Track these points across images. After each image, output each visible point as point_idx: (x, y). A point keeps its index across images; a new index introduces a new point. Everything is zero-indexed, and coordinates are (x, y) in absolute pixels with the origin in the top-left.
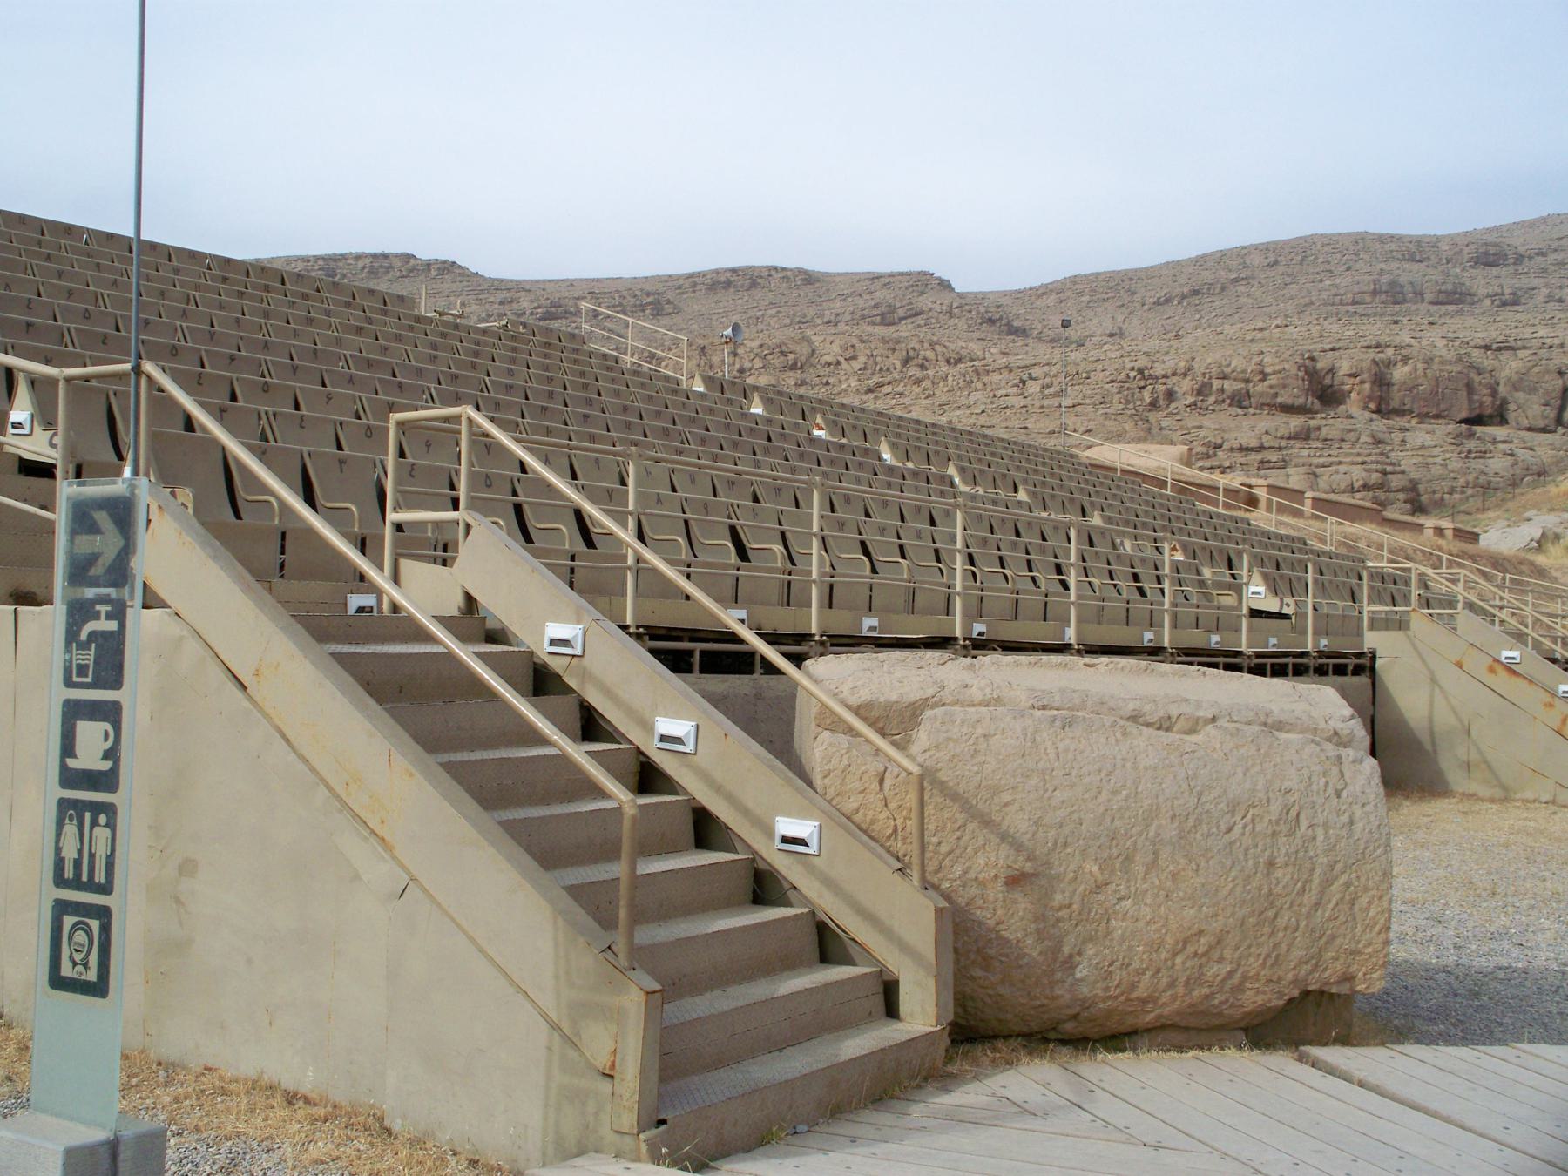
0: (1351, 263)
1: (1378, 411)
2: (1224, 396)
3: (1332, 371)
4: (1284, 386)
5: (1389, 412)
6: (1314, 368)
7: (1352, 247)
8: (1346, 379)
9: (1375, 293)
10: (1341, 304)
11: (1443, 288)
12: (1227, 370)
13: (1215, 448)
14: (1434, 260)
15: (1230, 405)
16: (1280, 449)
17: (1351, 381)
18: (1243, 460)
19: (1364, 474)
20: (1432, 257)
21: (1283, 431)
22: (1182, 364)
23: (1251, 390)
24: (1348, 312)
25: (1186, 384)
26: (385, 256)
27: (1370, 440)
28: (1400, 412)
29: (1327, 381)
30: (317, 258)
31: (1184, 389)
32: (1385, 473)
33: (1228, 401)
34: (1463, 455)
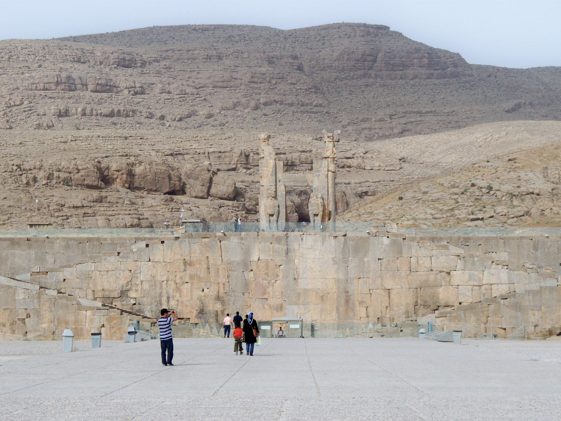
0: (41, 62)
1: (129, 188)
2: (60, 180)
3: (108, 168)
4: (88, 176)
5: (134, 188)
6: (100, 166)
7: (41, 51)
8: (115, 172)
9: (58, 84)
10: (36, 90)
11: (100, 82)
12: (60, 167)
13: (61, 206)
14: (92, 62)
15: (63, 184)
16: (91, 207)
17: (117, 173)
18: (76, 213)
19: (131, 220)
20: (91, 60)
21: (90, 198)
22: (38, 163)
23: (72, 177)
24: (41, 95)
25: (41, 175)
27: (129, 203)
28: (139, 189)
29: (106, 173)
31: (41, 176)
32: (139, 219)
33: (62, 183)
34: (170, 210)
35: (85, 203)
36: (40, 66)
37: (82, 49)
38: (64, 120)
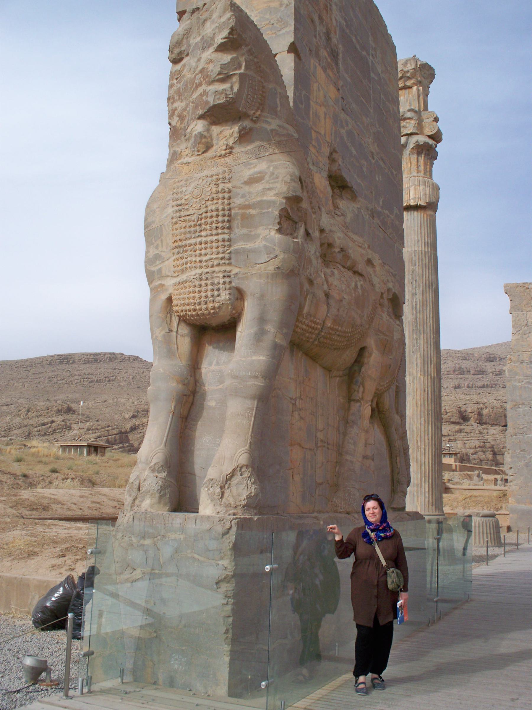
0: (446, 361)
1: (479, 423)
3: (466, 411)
4: (453, 416)
5: (482, 423)
8: (470, 414)
9: (454, 371)
11: (477, 369)
14: (473, 360)
16: (454, 435)
17: (471, 414)
19: (479, 443)
26: (114, 354)
27: (479, 433)
28: (485, 423)
29: (464, 414)
30: (91, 354)
32: (484, 443)
35: (450, 433)
36: (445, 363)
37: (468, 353)
38: (458, 390)
